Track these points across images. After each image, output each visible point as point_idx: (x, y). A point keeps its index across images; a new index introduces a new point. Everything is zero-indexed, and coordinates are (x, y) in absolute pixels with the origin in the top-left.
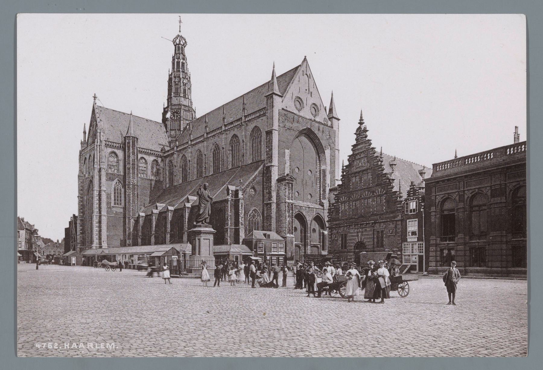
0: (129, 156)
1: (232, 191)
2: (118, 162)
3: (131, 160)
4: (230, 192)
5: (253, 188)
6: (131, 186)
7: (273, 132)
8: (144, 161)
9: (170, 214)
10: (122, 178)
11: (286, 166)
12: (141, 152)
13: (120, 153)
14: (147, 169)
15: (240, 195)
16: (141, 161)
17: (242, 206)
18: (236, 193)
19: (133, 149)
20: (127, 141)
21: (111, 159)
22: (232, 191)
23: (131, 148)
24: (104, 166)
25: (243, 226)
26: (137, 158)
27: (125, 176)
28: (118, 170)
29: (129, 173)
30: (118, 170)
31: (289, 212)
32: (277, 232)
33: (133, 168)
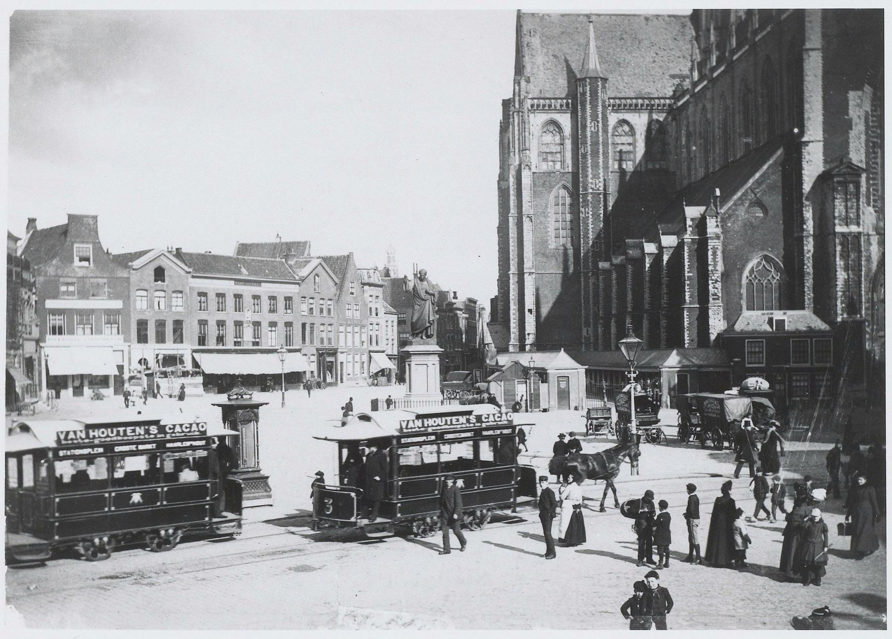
0: (584, 127)
1: (692, 220)
2: (563, 139)
3: (589, 134)
4: (689, 223)
5: (759, 203)
6: (589, 198)
7: (805, 56)
8: (626, 128)
9: (647, 260)
10: (570, 177)
11: (852, 134)
12: (617, 109)
13: (565, 120)
14: (635, 147)
15: (712, 227)
16: (620, 130)
17: (714, 254)
18: (701, 225)
19: (594, 107)
20: (580, 90)
21: (548, 138)
22: (692, 220)
23: (588, 106)
24: (533, 156)
25: (719, 302)
26: (605, 125)
27: (575, 175)
28: (563, 162)
29: (585, 168)
30: (563, 162)
31: (845, 256)
32: (816, 312)
33: (595, 154)
